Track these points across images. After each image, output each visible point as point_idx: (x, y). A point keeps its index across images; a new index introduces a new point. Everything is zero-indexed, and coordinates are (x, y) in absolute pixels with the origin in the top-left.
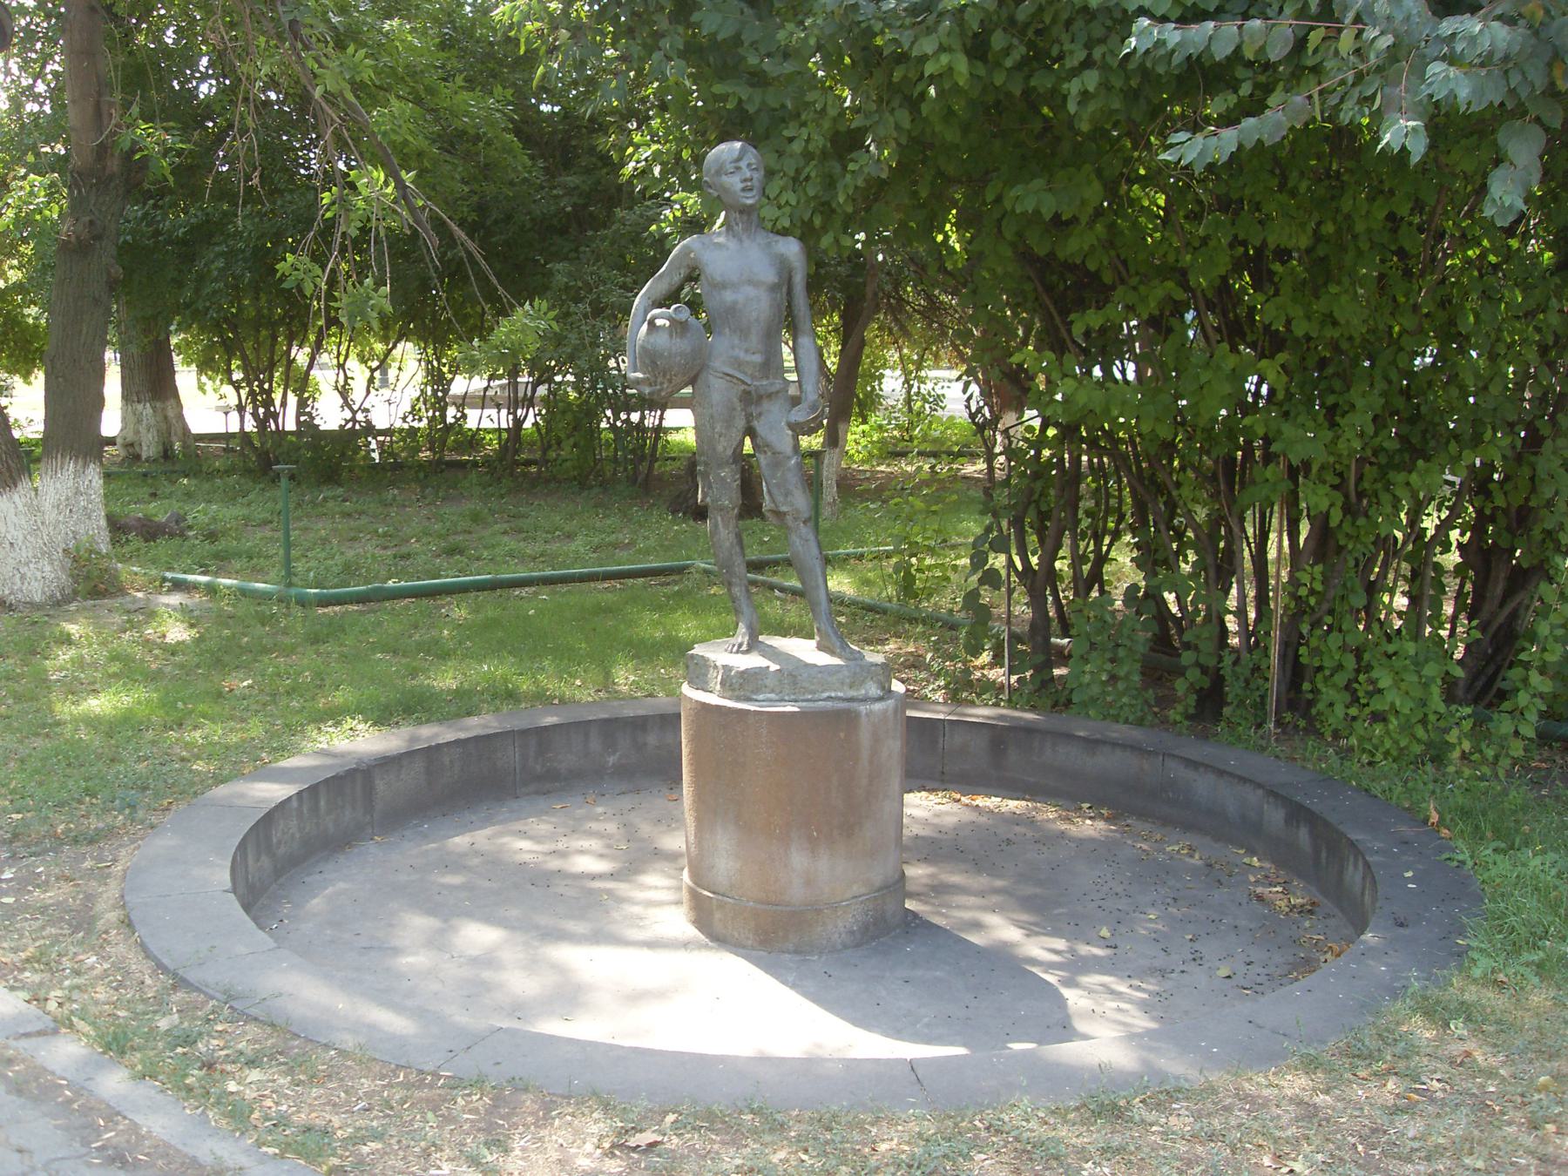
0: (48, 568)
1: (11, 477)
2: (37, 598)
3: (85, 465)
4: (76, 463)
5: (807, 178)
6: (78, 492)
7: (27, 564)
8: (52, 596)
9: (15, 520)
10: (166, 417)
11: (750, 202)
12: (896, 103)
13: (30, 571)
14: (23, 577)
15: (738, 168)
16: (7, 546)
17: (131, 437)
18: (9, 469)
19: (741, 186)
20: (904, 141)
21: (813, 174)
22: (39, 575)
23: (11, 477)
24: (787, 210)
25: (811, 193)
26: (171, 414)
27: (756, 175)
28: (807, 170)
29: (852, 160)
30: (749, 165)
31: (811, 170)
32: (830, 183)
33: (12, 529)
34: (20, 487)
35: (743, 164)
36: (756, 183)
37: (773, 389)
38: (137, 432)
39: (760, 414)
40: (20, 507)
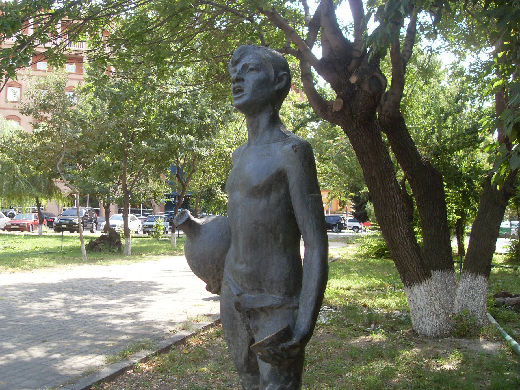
0: (435, 320)
1: (419, 278)
2: (429, 333)
3: (477, 276)
4: (472, 275)
6: (470, 288)
7: (425, 317)
8: (435, 333)
9: (421, 297)
13: (427, 321)
14: (423, 323)
16: (417, 308)
18: (418, 275)
22: (430, 323)
23: (420, 279)
33: (419, 301)
34: (424, 283)
37: (263, 305)
39: (257, 329)
40: (423, 291)
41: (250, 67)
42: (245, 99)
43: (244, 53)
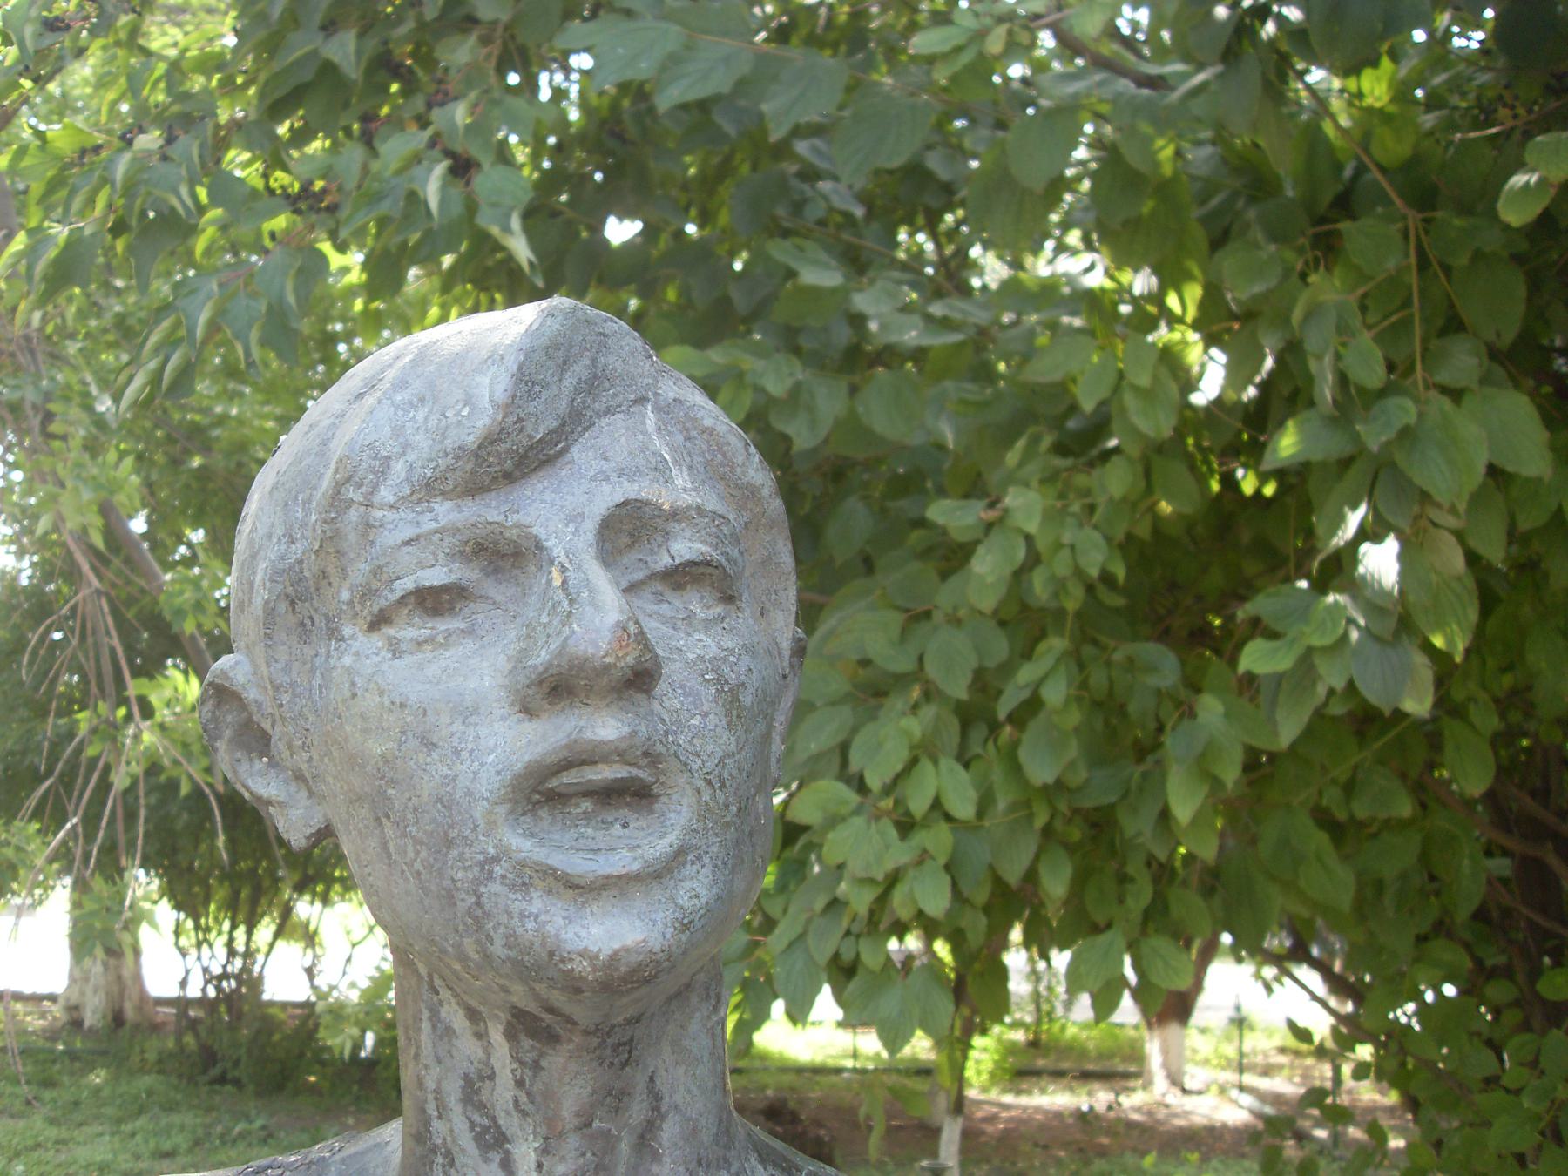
5: (1032, 705)
10: (119, 978)
11: (607, 934)
12: (1463, 362)
15: (505, 556)
17: (74, 1000)
19: (511, 742)
20: (1495, 552)
21: (1055, 693)
24: (939, 839)
25: (1041, 772)
26: (126, 973)
27: (700, 646)
28: (1026, 674)
29: (1256, 627)
30: (626, 529)
31: (1047, 675)
32: (1126, 739)
35: (559, 513)
36: (691, 716)
38: (82, 993)
41: (685, 547)
42: (696, 888)
43: (593, 384)
